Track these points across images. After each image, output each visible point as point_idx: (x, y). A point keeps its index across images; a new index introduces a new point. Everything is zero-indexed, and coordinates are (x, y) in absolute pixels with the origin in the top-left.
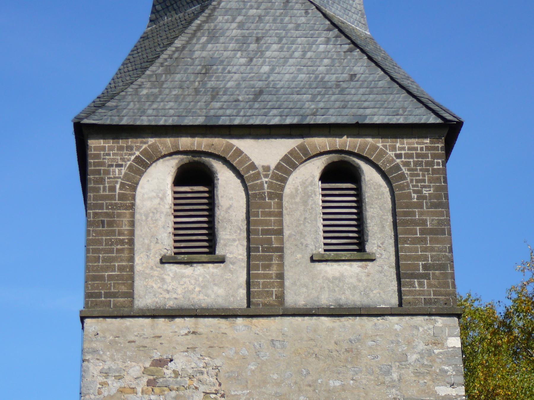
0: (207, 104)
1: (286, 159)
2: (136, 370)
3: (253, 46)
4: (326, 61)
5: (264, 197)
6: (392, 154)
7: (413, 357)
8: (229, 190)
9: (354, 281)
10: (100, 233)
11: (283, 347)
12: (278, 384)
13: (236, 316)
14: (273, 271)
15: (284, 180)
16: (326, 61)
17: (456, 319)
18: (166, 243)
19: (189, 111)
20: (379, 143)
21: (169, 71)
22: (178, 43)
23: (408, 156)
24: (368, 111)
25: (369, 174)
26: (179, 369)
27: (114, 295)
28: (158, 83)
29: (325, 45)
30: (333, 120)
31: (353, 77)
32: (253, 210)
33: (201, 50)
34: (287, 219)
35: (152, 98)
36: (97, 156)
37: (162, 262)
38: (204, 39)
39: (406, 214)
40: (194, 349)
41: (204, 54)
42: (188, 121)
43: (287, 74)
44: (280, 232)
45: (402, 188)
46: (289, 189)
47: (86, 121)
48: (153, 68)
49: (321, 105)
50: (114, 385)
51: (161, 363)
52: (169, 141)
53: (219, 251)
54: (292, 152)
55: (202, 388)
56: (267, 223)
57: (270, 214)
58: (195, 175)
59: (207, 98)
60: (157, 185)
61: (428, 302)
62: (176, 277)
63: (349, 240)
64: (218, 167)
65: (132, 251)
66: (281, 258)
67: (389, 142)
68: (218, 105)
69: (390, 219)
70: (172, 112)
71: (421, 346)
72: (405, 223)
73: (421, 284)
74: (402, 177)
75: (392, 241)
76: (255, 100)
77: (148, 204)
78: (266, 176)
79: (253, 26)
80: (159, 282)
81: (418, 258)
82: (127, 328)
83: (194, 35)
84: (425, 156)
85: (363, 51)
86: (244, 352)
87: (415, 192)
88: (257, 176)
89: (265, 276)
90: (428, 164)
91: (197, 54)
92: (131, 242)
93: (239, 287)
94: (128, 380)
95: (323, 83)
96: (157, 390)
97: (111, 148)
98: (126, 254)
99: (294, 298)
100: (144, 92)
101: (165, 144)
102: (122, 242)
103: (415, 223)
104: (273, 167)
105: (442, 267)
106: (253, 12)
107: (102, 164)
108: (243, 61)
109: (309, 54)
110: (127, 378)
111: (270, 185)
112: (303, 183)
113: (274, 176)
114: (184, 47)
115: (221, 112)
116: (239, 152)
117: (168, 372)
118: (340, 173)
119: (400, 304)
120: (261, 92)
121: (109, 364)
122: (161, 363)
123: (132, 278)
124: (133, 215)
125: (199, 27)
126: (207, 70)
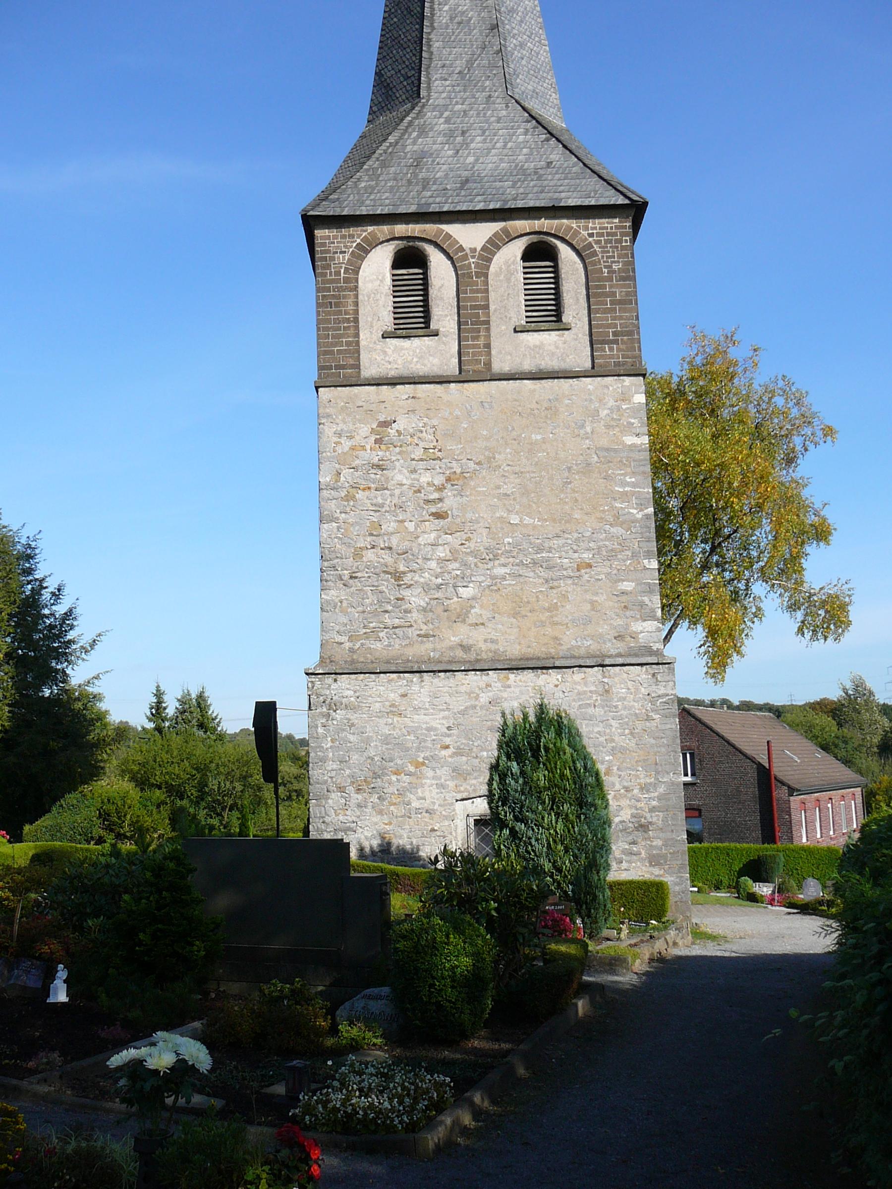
0: (419, 193)
1: (490, 241)
2: (364, 430)
3: (459, 139)
4: (525, 151)
5: (472, 277)
6: (585, 233)
7: (604, 413)
8: (440, 270)
9: (552, 348)
10: (329, 313)
11: (491, 407)
12: (487, 439)
13: (450, 382)
14: (481, 342)
15: (489, 260)
16: (525, 151)
17: (641, 378)
18: (387, 320)
19: (403, 201)
20: (574, 224)
21: (384, 165)
22: (391, 139)
23: (599, 235)
24: (563, 195)
25: (565, 253)
26: (401, 429)
27: (343, 367)
28: (374, 176)
29: (525, 137)
30: (531, 204)
31: (549, 164)
32: (462, 288)
33: (413, 144)
34: (492, 296)
35: (370, 190)
36: (324, 245)
37: (383, 337)
38: (415, 134)
39: (597, 287)
40: (413, 411)
41: (415, 148)
42: (402, 209)
43: (490, 164)
44: (487, 307)
45: (594, 264)
46: (493, 268)
47: (311, 213)
48: (370, 163)
49: (521, 190)
50: (346, 444)
51: (386, 424)
52: (385, 228)
53: (433, 326)
54: (496, 234)
55: (422, 444)
56: (476, 299)
57: (477, 291)
58: (410, 258)
59: (419, 188)
60: (377, 269)
61: (617, 364)
62: (396, 349)
63: (549, 313)
64: (430, 249)
65: (357, 328)
66: (488, 330)
67: (582, 223)
68: (429, 194)
69: (584, 292)
70: (387, 201)
71: (611, 403)
72: (597, 295)
73: (611, 349)
74: (595, 254)
75: (586, 312)
76: (461, 188)
77: (370, 286)
78: (473, 257)
79: (459, 120)
80: (381, 354)
81: (609, 326)
82: (356, 395)
83: (406, 131)
84: (615, 234)
85: (558, 140)
86: (457, 412)
87: (605, 267)
88: (466, 257)
89: (474, 346)
90: (617, 241)
91: (409, 148)
92: (356, 320)
93: (452, 356)
94: (358, 440)
95: (523, 171)
96: (383, 447)
97: (335, 237)
98: (352, 331)
99: (500, 365)
100: (363, 185)
101: (382, 232)
102: (348, 321)
103: (607, 295)
104: (479, 249)
105: (630, 333)
106: (458, 107)
107: (328, 252)
108: (450, 153)
109: (509, 145)
110: (357, 438)
111: (477, 265)
112: (506, 263)
113: (481, 257)
114: (397, 143)
115: (431, 200)
116: (448, 236)
117: (392, 431)
118: (540, 253)
119: (593, 367)
120: (467, 181)
121: (342, 426)
122: (386, 424)
123: (358, 352)
124: (357, 296)
125: (410, 123)
126: (418, 161)
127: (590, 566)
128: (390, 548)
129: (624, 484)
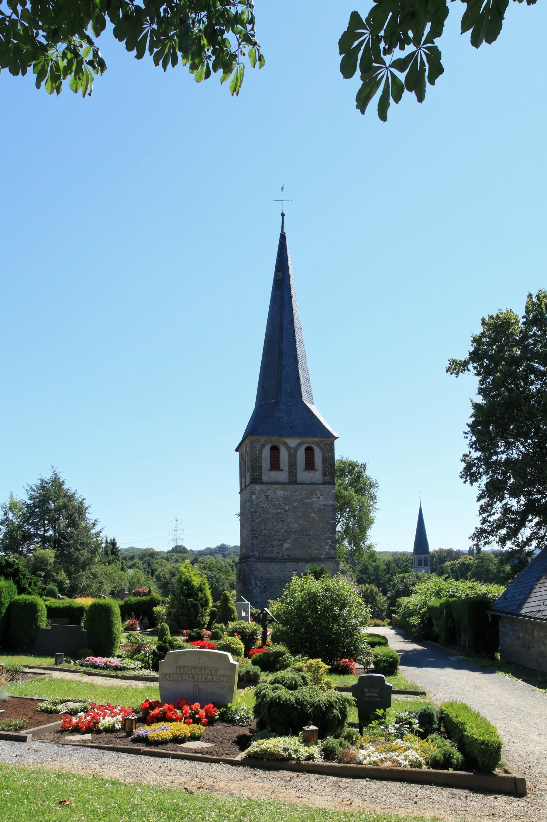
3: (289, 414)
8: (284, 454)
22: (271, 413)
80: (268, 475)
129: (329, 514)
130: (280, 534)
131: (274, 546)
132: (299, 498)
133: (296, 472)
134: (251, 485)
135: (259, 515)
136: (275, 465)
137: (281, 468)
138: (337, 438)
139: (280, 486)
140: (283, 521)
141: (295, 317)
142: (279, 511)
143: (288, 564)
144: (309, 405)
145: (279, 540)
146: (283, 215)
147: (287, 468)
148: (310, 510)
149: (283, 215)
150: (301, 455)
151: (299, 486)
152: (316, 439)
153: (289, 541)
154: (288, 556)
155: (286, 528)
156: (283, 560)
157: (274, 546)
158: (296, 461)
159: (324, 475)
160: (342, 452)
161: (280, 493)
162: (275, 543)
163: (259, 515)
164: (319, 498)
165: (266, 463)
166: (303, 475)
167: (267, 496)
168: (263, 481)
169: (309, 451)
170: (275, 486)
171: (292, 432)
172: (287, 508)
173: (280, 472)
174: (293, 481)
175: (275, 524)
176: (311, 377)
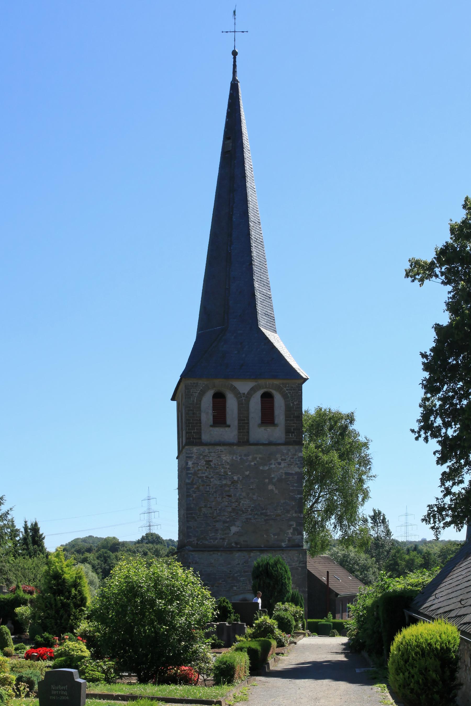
8: (232, 404)
27: (195, 439)
73: (292, 436)
78: (244, 397)
87: (292, 403)
127: (280, 515)
128: (211, 507)
130: (226, 514)
131: (217, 530)
132: (253, 464)
133: (248, 429)
134: (186, 447)
135: (198, 488)
136: (220, 419)
137: (228, 422)
138: (305, 380)
139: (225, 447)
140: (229, 496)
141: (251, 205)
142: (224, 482)
143: (237, 555)
144: (268, 333)
145: (225, 522)
146: (235, 54)
147: (236, 423)
148: (267, 481)
149: (235, 54)
150: (255, 404)
151: (252, 447)
152: (276, 382)
153: (238, 523)
154: (236, 543)
155: (234, 505)
156: (230, 549)
157: (217, 530)
158: (248, 414)
159: (288, 431)
160: (311, 403)
161: (226, 458)
162: (219, 525)
163: (198, 488)
164: (279, 464)
165: (207, 416)
166: (258, 433)
167: (208, 462)
168: (203, 441)
169: (267, 398)
170: (219, 448)
171: (244, 373)
172: (235, 478)
173: (227, 429)
174: (244, 441)
175: (219, 500)
176: (273, 293)
